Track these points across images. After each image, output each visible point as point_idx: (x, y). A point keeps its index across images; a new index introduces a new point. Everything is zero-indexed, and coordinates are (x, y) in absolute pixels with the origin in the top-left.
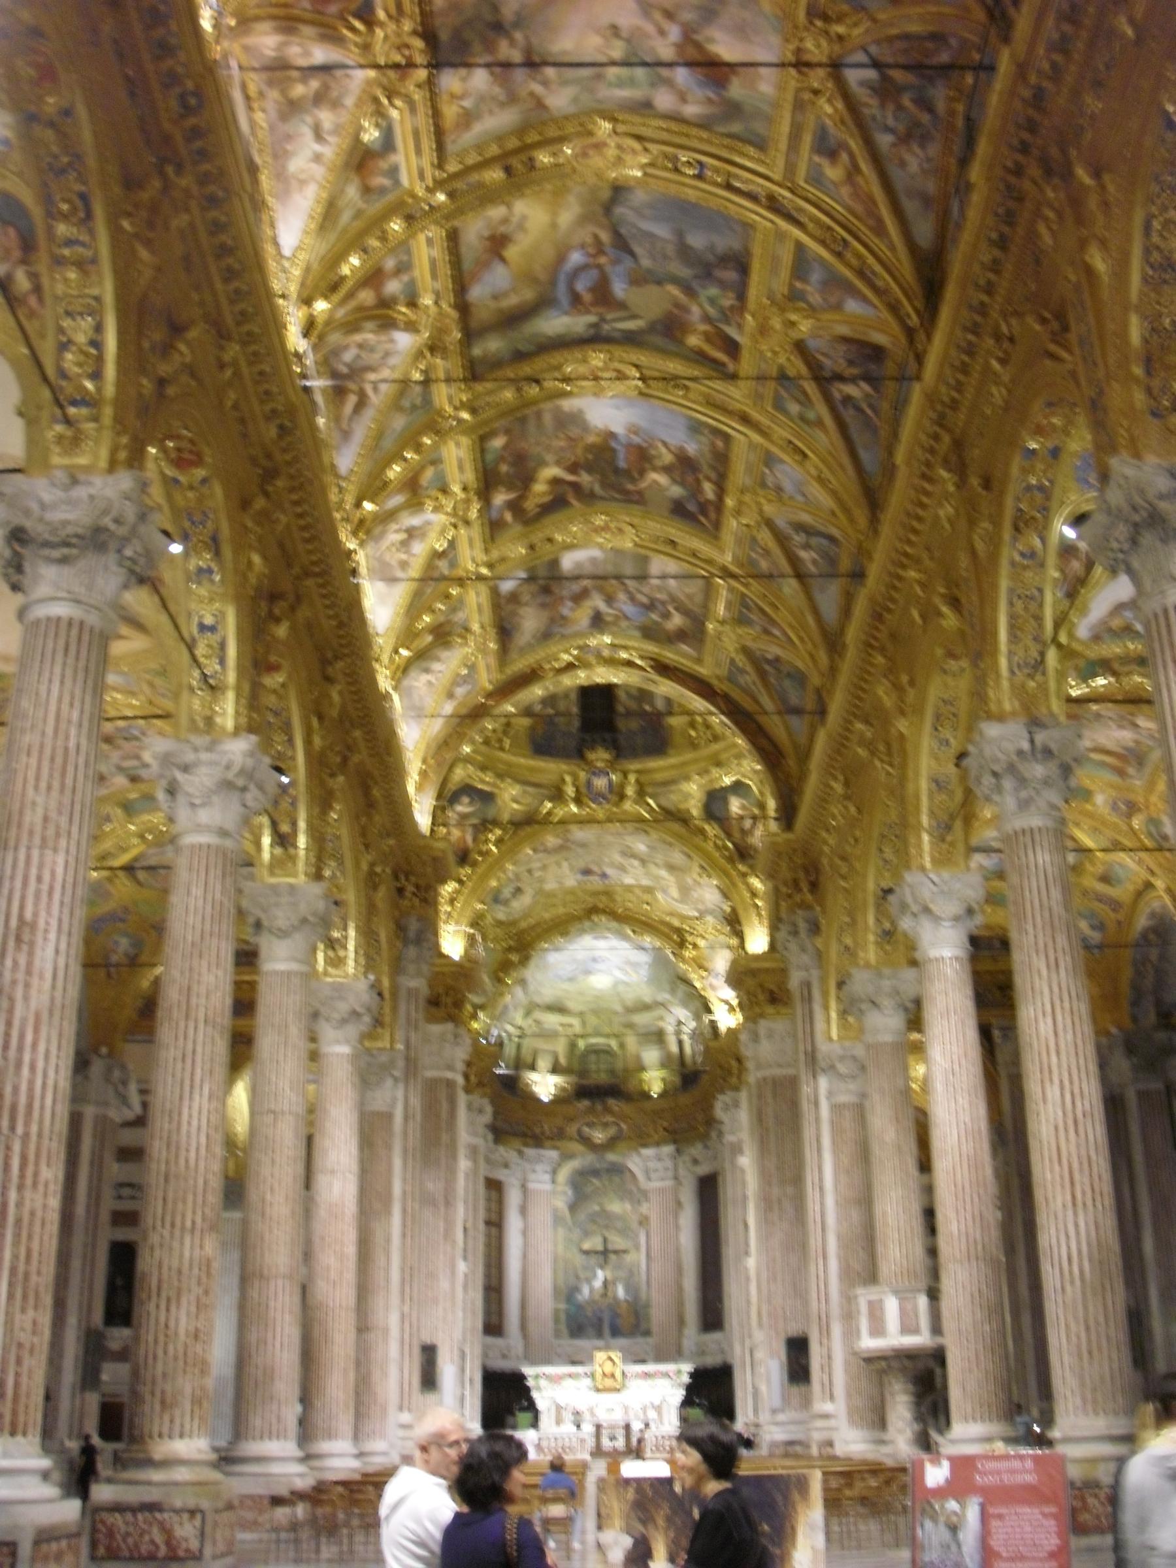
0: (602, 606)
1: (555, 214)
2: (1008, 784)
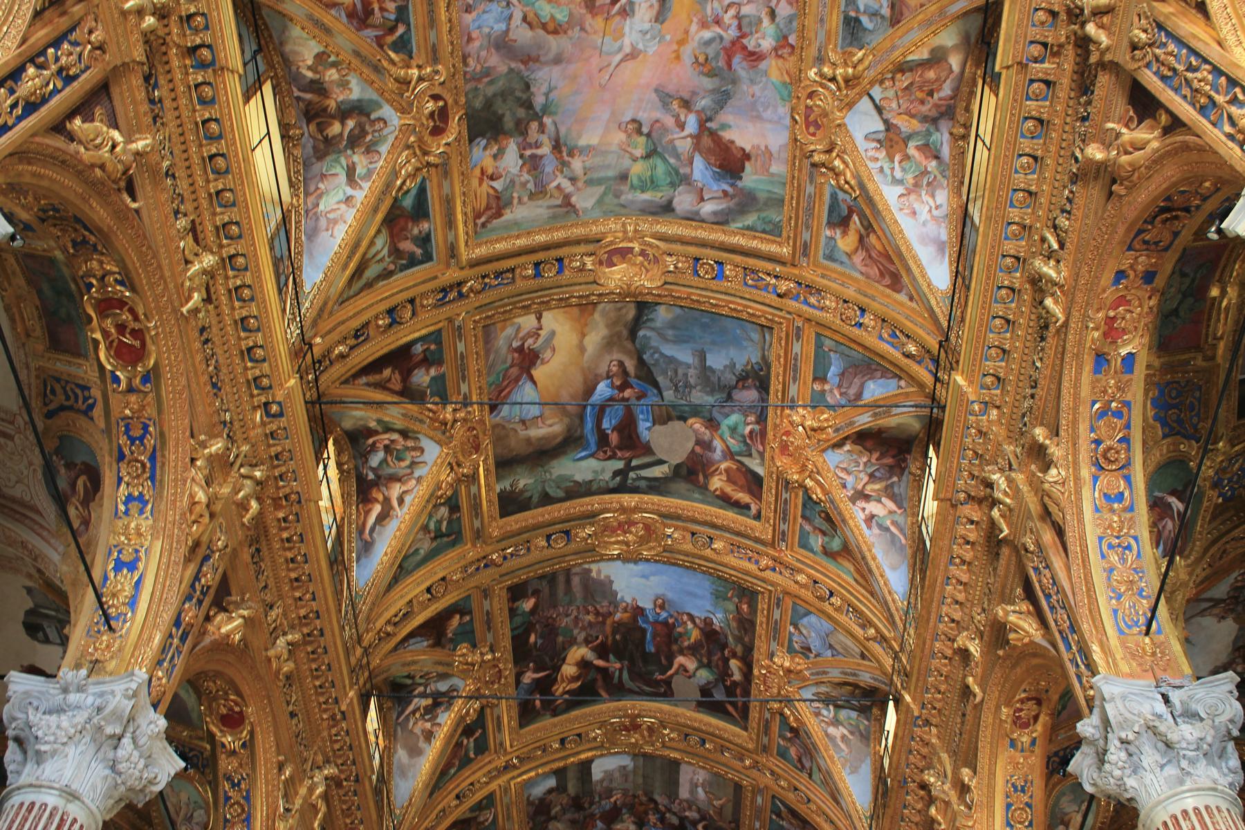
1: (583, 335)
2: (1150, 756)
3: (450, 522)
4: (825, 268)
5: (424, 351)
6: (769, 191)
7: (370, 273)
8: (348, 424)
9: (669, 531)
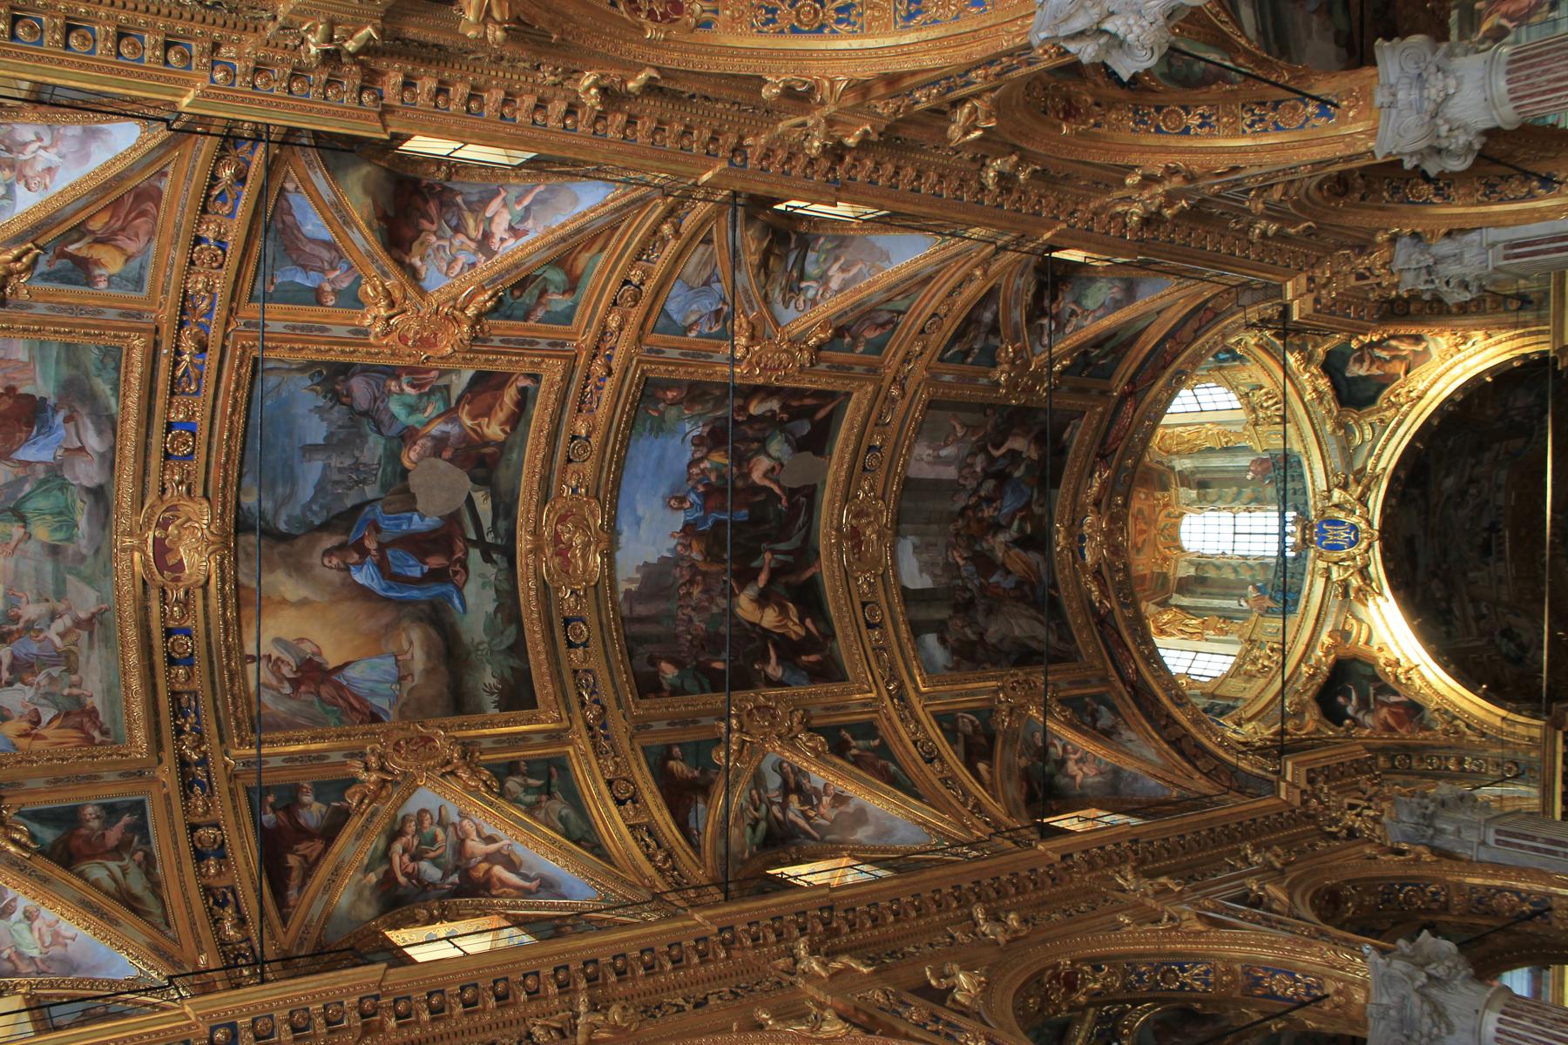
0: (1002, 537)
3: (531, 774)
4: (153, 289)
5: (274, 810)
6: (57, 363)
7: (137, 884)
8: (367, 911)
9: (567, 492)
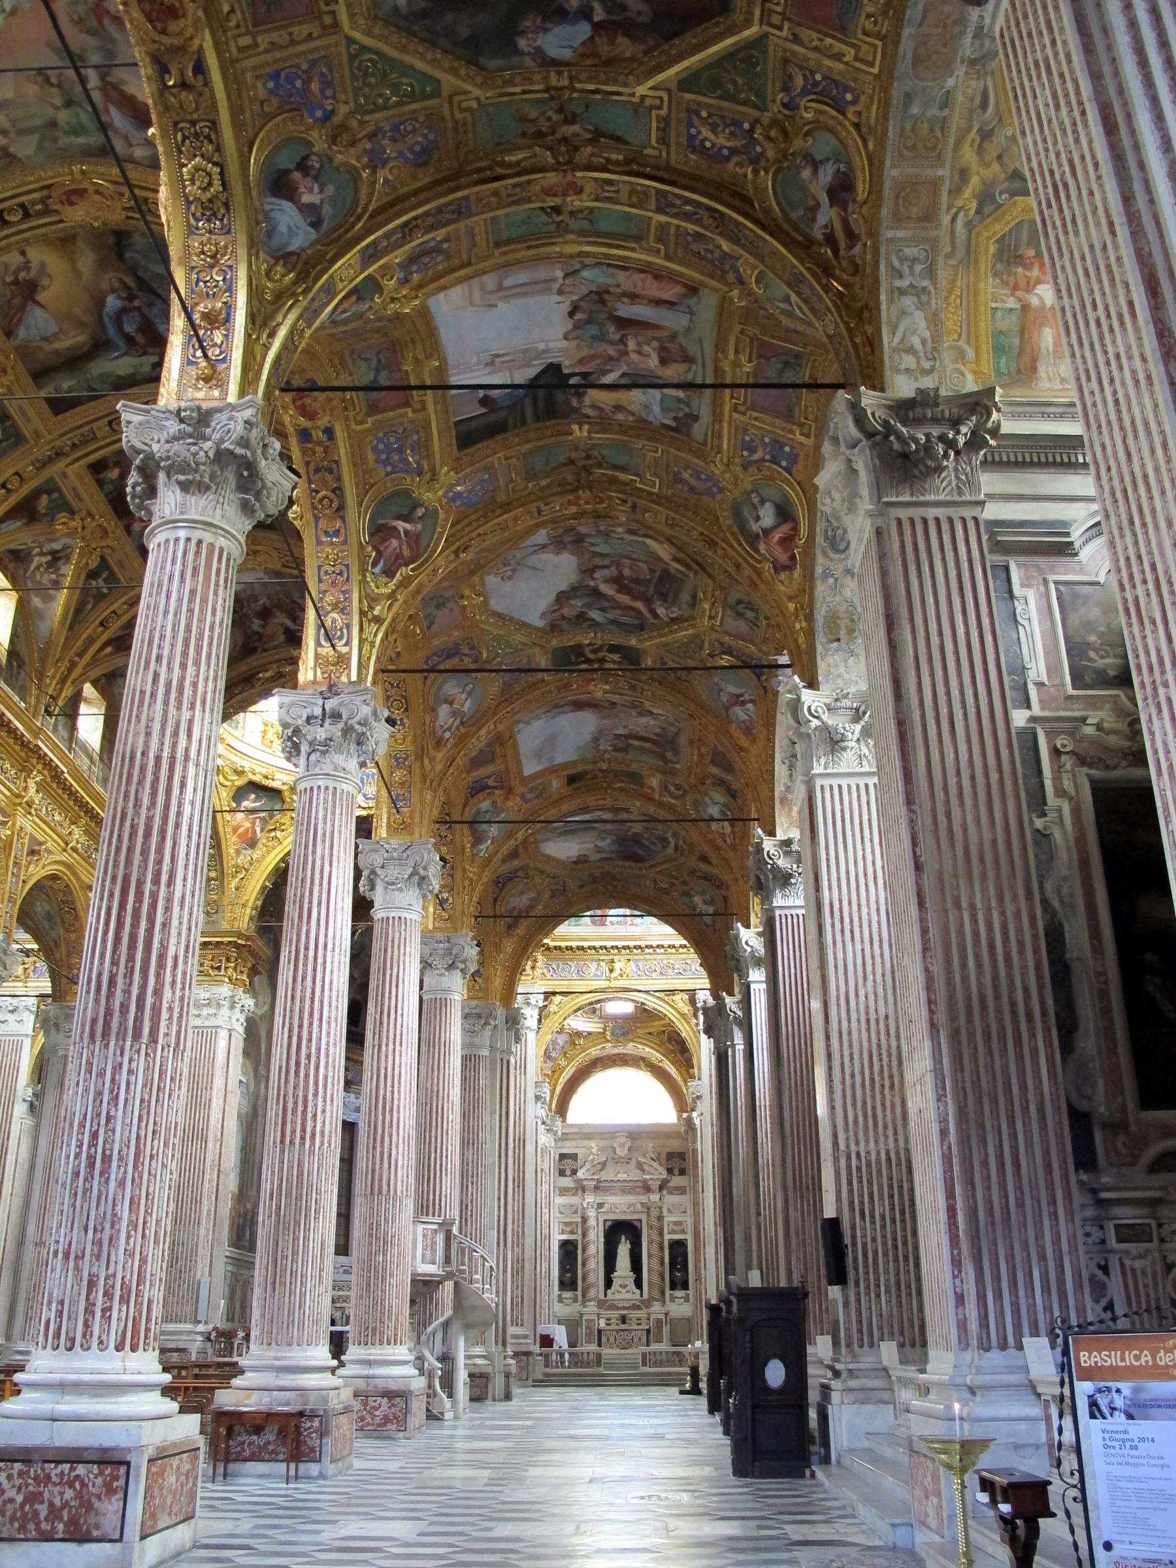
0: (288, 623)
1: (73, 263)
